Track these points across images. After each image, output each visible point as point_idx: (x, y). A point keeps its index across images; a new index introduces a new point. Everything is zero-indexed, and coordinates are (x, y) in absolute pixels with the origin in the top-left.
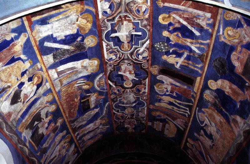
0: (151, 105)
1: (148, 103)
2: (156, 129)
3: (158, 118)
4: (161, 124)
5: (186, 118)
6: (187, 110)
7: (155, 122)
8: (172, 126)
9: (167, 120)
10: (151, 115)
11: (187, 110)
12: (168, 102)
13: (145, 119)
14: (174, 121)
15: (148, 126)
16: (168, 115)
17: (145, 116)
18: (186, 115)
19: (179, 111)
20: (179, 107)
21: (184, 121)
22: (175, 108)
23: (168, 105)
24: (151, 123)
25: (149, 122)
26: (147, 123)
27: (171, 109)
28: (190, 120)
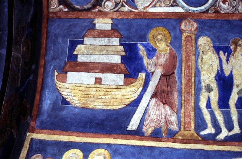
0: (195, 25)
1: (204, 17)
2: (79, 47)
3: (140, 47)
4: (117, 59)
5: (193, 132)
6: (230, 128)
7: (116, 41)
8: (131, 92)
9: (144, 75)
10: (149, 27)
11: (230, 128)
12: (227, 73)
13: (127, 8)
14: (154, 95)
15: (93, 20)
16: (167, 76)
17: (140, 8)
18: (205, 127)
19: (209, 106)
20: (223, 103)
21: (174, 127)
22: (215, 96)
23: (214, 74)
24: (110, 28)
25: (110, 21)
26: (103, 14)
27: (203, 84)
28: (196, 142)
